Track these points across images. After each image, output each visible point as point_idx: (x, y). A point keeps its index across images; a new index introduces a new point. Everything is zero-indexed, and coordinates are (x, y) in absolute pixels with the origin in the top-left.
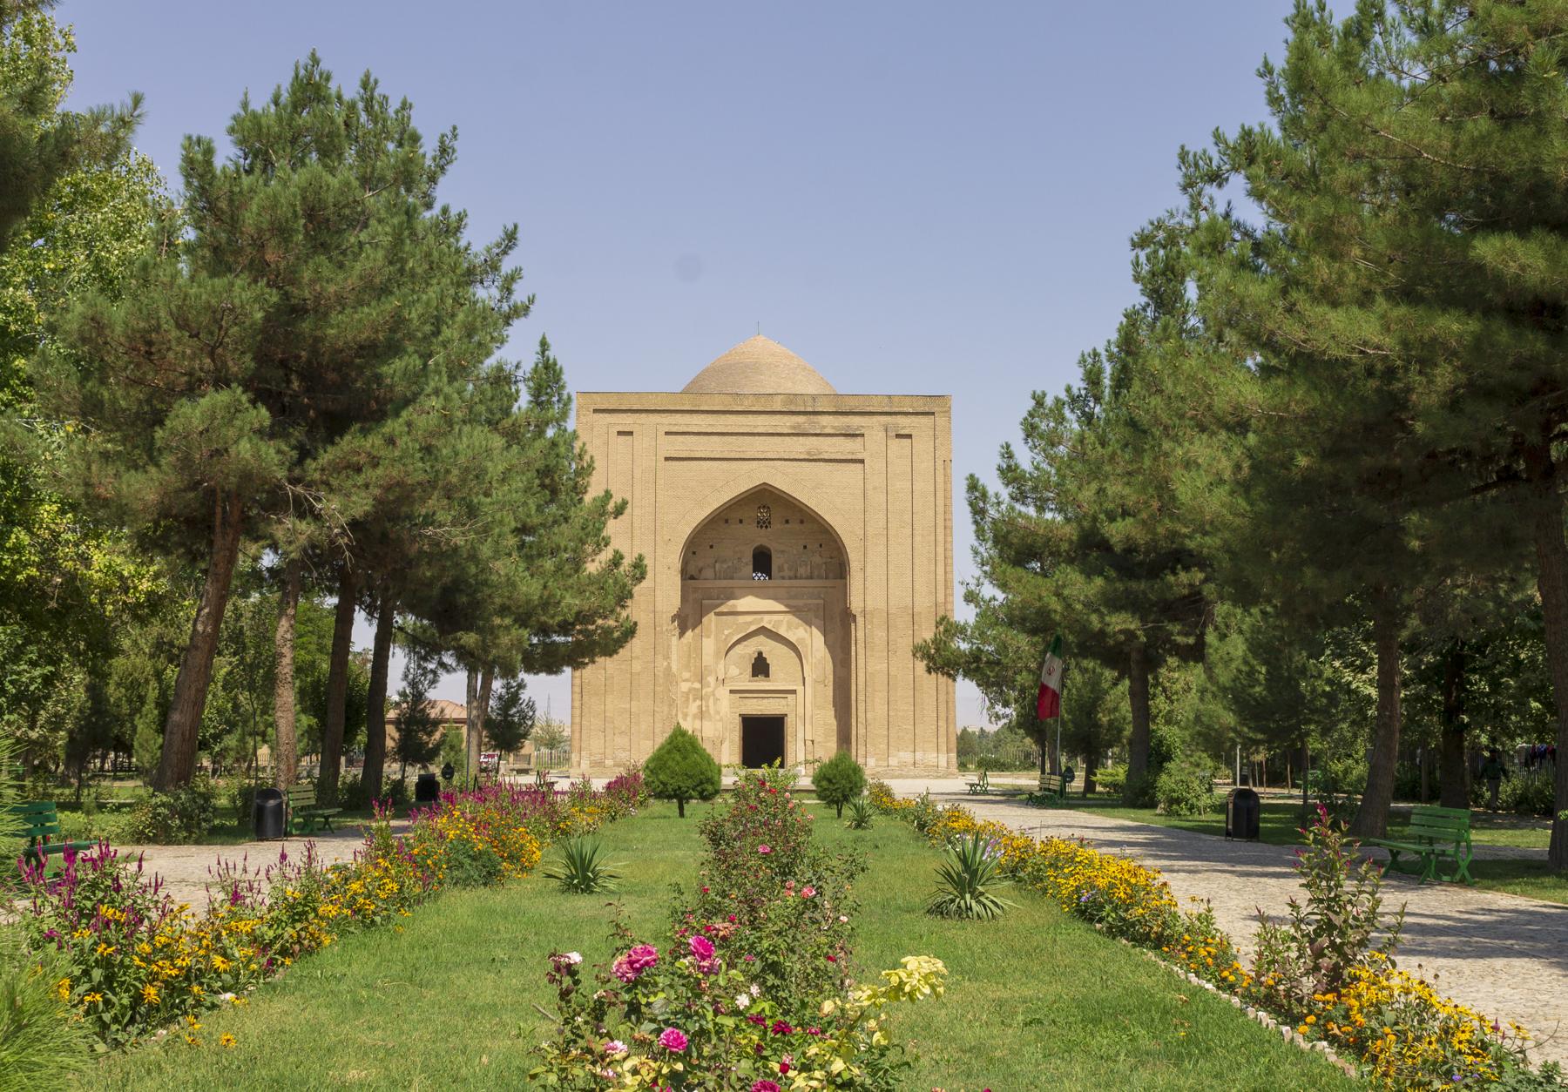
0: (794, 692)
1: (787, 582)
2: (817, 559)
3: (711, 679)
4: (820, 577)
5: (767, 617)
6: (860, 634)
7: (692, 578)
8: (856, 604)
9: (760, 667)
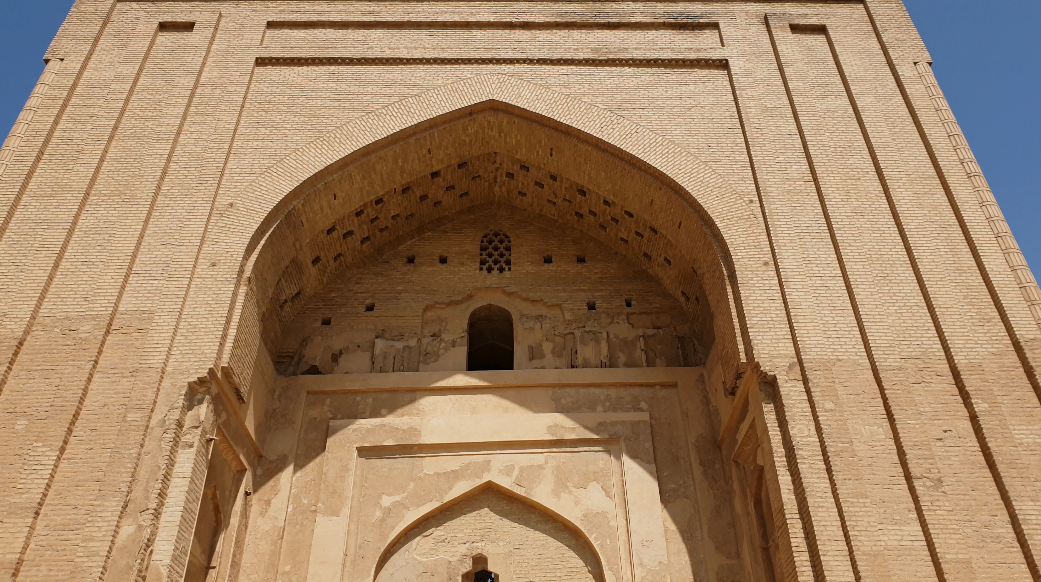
1: (551, 376)
2: (623, 330)
5: (499, 459)
6: (802, 431)
7: (314, 370)
8: (770, 349)
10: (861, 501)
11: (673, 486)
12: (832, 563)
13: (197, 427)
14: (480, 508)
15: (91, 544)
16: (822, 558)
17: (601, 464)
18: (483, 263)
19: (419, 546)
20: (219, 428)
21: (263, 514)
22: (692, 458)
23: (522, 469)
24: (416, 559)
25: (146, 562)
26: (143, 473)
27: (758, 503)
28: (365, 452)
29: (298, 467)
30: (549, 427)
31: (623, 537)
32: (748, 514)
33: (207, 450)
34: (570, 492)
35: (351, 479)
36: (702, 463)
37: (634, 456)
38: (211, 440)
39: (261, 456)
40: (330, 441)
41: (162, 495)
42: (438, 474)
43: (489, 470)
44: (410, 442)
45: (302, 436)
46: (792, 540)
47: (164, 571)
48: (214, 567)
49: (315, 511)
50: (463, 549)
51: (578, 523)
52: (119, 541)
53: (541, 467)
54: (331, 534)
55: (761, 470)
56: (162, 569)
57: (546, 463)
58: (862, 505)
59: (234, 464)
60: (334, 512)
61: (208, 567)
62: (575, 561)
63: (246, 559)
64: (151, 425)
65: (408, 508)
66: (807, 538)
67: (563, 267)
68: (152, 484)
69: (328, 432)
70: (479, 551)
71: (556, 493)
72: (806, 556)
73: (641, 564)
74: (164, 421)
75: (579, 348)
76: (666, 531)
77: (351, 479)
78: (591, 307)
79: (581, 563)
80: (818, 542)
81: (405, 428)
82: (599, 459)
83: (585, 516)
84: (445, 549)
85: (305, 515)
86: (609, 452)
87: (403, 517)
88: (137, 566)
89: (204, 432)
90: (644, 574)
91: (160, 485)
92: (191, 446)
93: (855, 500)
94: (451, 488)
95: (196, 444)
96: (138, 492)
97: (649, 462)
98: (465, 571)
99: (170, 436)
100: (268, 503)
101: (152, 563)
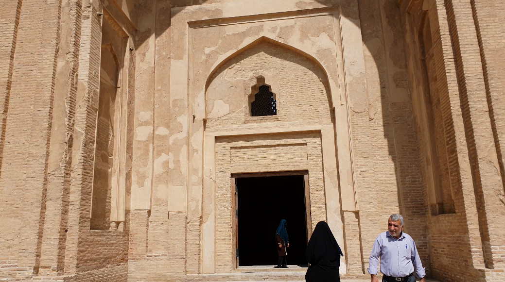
0: (317, 133)
3: (184, 120)
5: (268, 24)
9: (262, 102)
10: (492, 19)
11: (369, 31)
12: (468, 58)
13: (89, 7)
14: (259, 52)
15: (43, 71)
16: (462, 55)
17: (327, 22)
19: (227, 74)
20: (104, 10)
21: (142, 61)
22: (382, 14)
23: (281, 29)
24: (226, 80)
25: (75, 81)
26: (63, 32)
27: (421, 35)
28: (194, 25)
29: (157, 35)
30: (297, 3)
31: (340, 62)
32: (414, 42)
33: (99, 21)
34: (310, 39)
35: (186, 40)
36: (387, 17)
37: (347, 16)
38: (100, 15)
39: (137, 30)
40: (173, 20)
41: (76, 44)
42: (234, 34)
43: (263, 31)
44: (217, 17)
45: (157, 18)
46: (443, 47)
47: (86, 85)
48: (119, 87)
49: (170, 58)
50: (251, 74)
51: (314, 56)
52: (58, 69)
53: (292, 27)
54: (179, 70)
55: (425, 13)
56: (84, 83)
57: (295, 24)
58: (492, 21)
59: (120, 33)
60: (180, 58)
61: (117, 88)
62: (312, 75)
63: (137, 84)
64: (62, 6)
65: (219, 54)
66: (453, 45)
68: (69, 38)
69: (171, 15)
70: (260, 74)
71: (301, 40)
72: (451, 56)
73: (350, 75)
74: (69, 3)
76: (365, 56)
77: (186, 40)
79: (316, 77)
80: (461, 46)
81: (213, 10)
82: (327, 20)
83: (318, 51)
84: (241, 74)
85: (164, 61)
86: (332, 15)
87: (217, 58)
88: (70, 82)
89: (94, 10)
90: (351, 80)
91: (74, 39)
92: (88, 18)
93: (488, 19)
94: (242, 42)
95: (91, 16)
96: (62, 43)
97: (356, 19)
98: (253, 85)
99: (74, 12)
100: (144, 55)
101: (79, 81)
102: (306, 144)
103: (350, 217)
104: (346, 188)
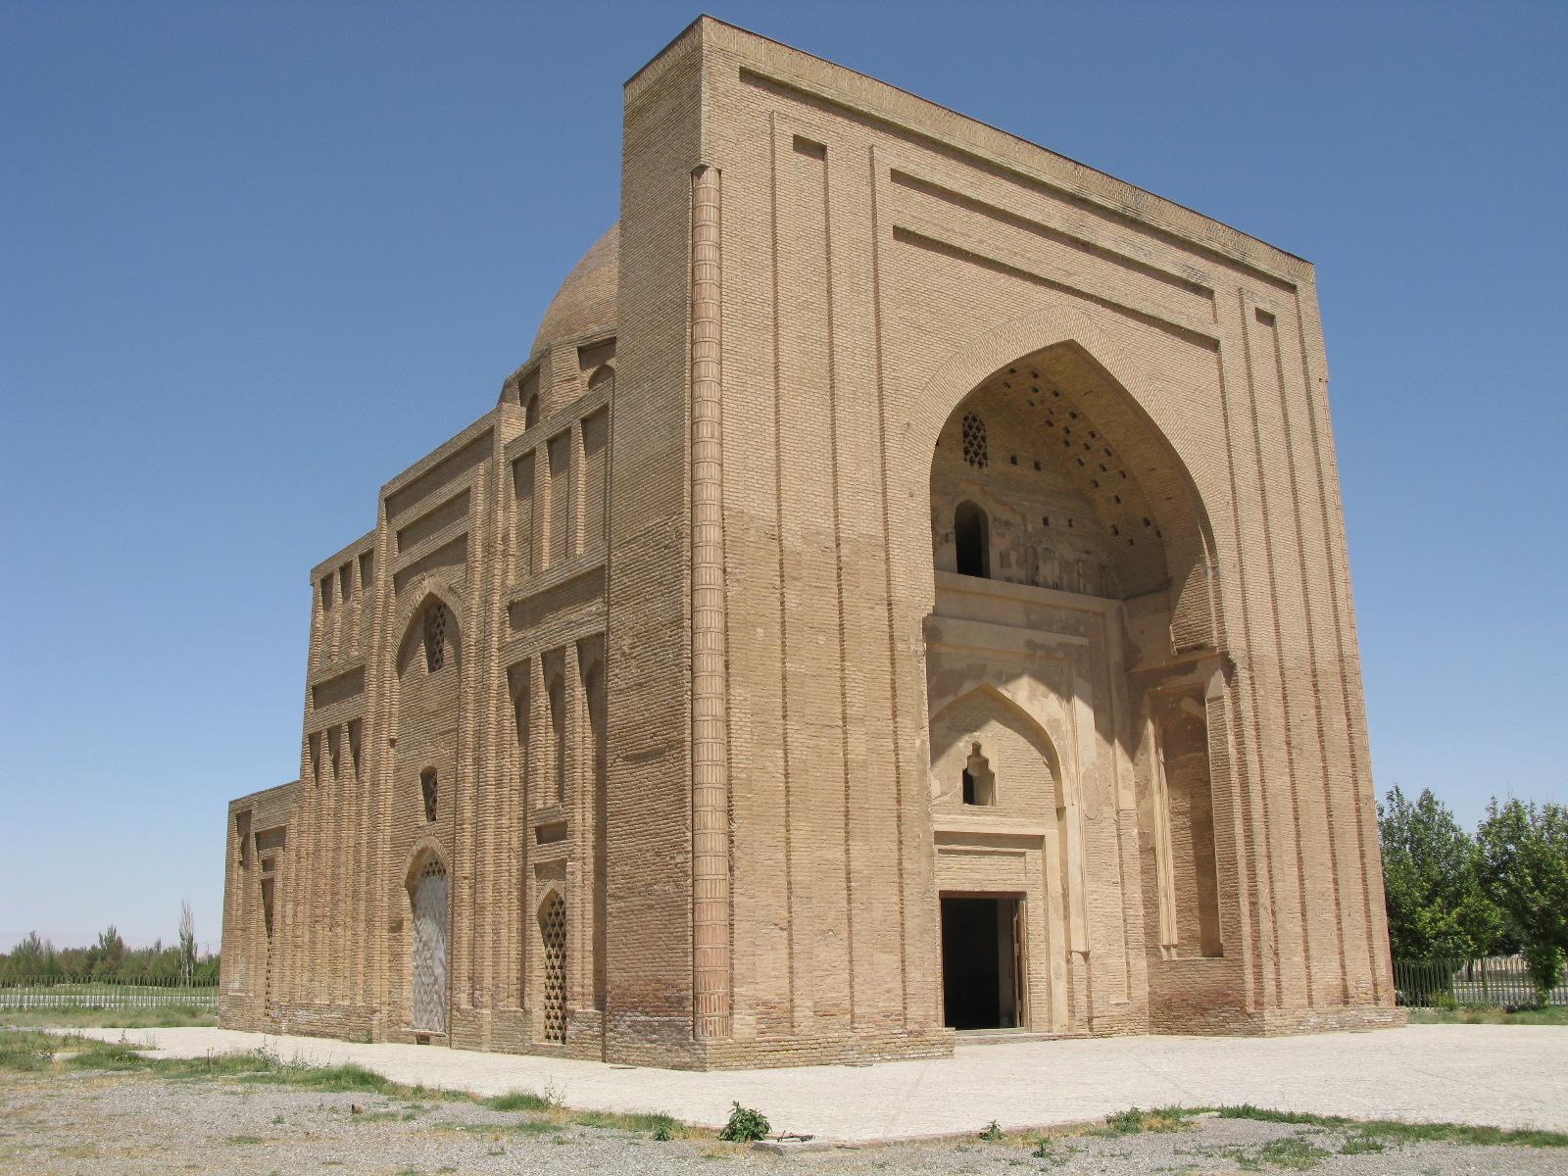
0: (1037, 842)
4: (1074, 589)
6: (1246, 706)
18: (967, 452)
34: (1039, 700)
67: (1024, 471)
75: (1041, 563)
78: (1046, 521)
102: (1024, 854)
103: (1077, 959)
104: (1076, 921)
